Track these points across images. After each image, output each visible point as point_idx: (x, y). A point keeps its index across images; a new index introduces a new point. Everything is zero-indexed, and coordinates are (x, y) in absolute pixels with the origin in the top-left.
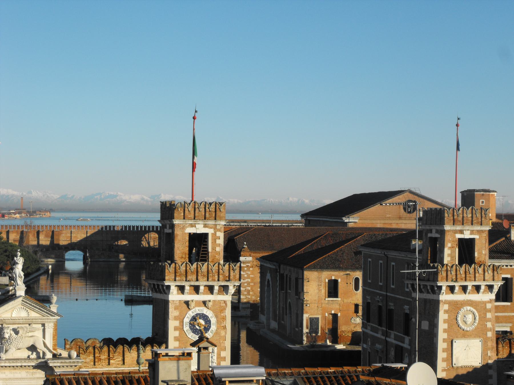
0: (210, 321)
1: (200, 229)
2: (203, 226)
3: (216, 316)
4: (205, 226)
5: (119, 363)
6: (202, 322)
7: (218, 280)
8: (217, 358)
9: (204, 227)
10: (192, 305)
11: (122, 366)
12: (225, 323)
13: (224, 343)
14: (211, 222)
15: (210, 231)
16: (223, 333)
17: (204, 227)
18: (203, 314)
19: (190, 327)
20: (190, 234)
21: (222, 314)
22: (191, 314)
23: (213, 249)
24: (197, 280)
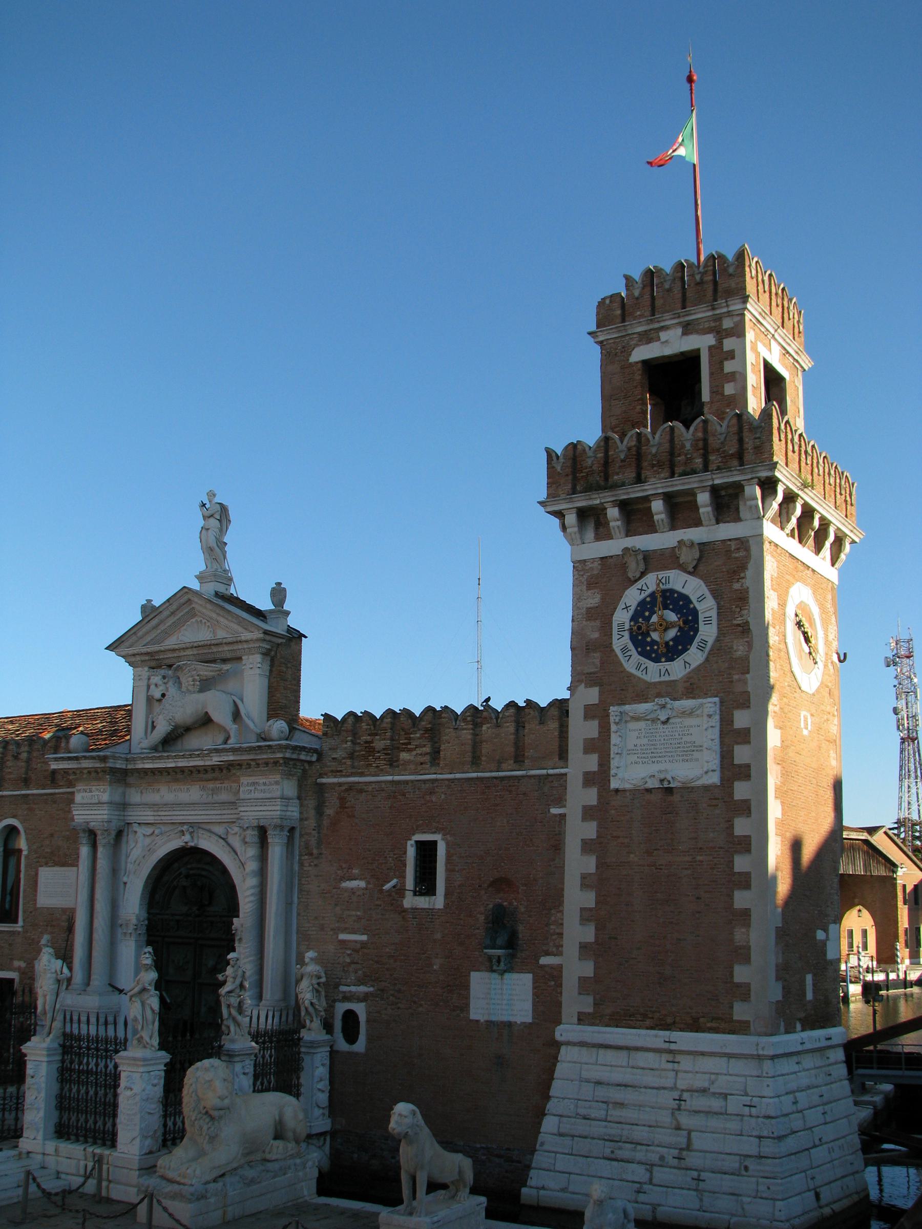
0: (695, 613)
1: (672, 343)
2: (679, 331)
3: (716, 594)
4: (688, 328)
5: (422, 759)
6: (672, 617)
7: (706, 469)
8: (722, 735)
9: (685, 333)
10: (633, 569)
11: (433, 770)
12: (745, 612)
13: (745, 682)
14: (701, 313)
15: (702, 342)
16: (739, 649)
17: (685, 333)
18: (672, 591)
19: (633, 638)
20: (645, 363)
21: (736, 586)
22: (632, 597)
23: (712, 392)
24: (639, 480)
